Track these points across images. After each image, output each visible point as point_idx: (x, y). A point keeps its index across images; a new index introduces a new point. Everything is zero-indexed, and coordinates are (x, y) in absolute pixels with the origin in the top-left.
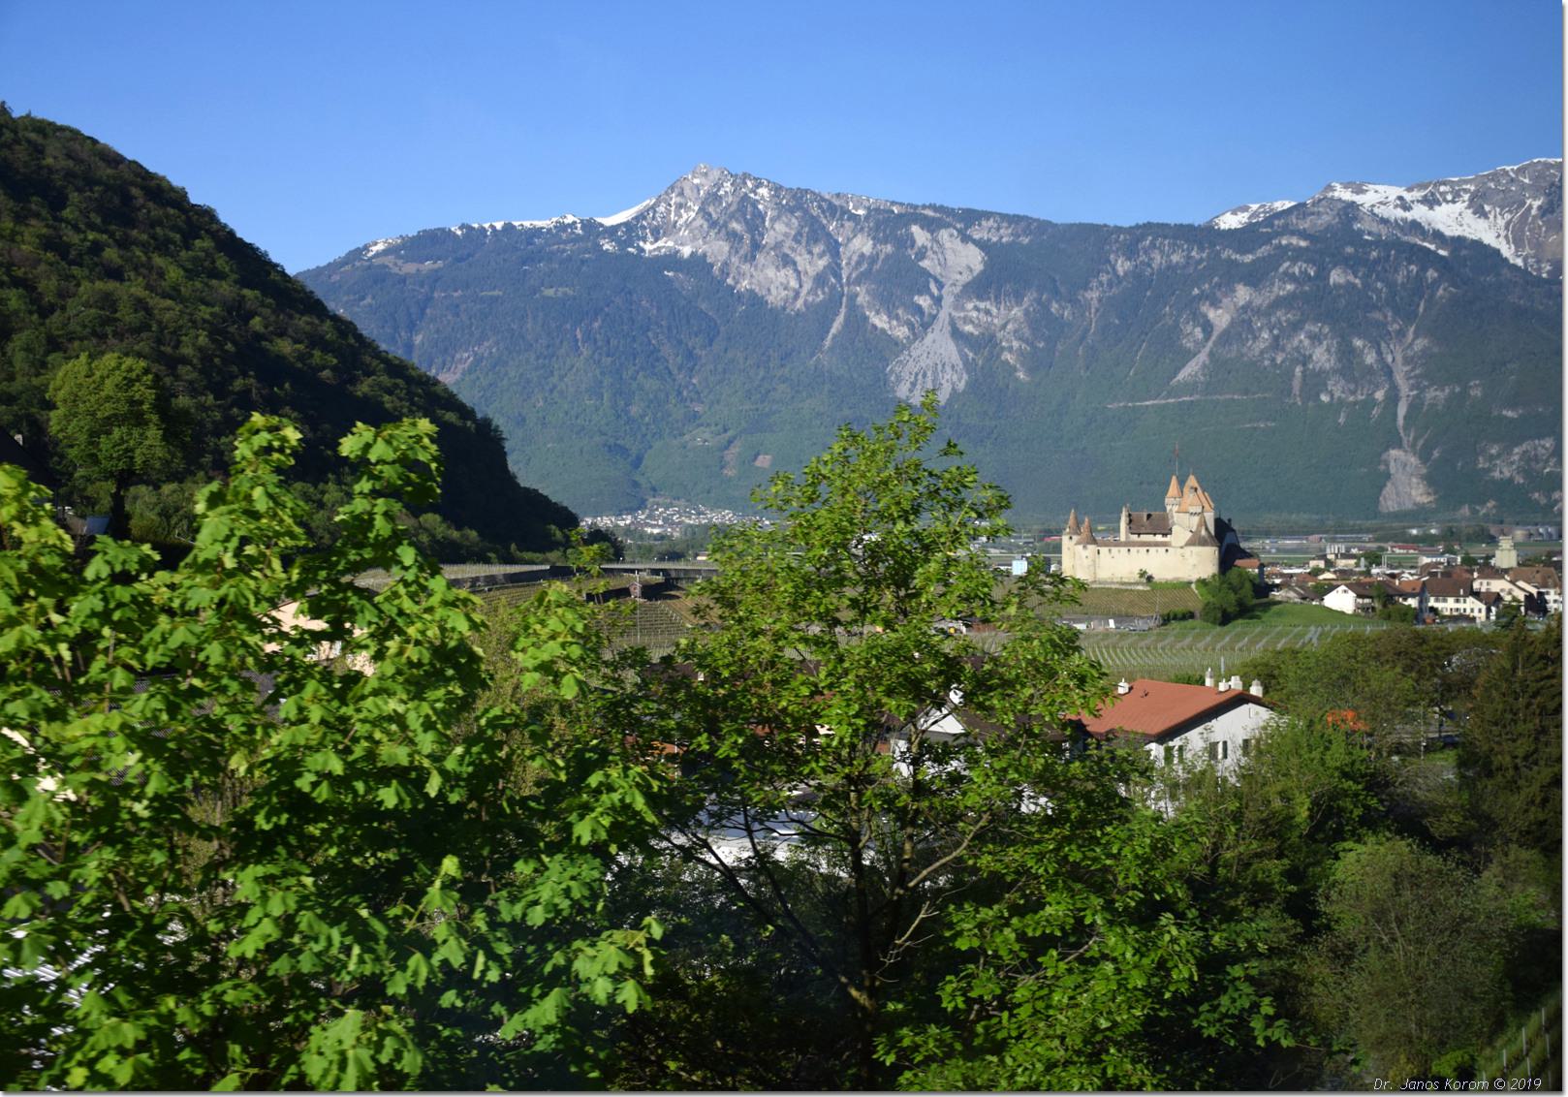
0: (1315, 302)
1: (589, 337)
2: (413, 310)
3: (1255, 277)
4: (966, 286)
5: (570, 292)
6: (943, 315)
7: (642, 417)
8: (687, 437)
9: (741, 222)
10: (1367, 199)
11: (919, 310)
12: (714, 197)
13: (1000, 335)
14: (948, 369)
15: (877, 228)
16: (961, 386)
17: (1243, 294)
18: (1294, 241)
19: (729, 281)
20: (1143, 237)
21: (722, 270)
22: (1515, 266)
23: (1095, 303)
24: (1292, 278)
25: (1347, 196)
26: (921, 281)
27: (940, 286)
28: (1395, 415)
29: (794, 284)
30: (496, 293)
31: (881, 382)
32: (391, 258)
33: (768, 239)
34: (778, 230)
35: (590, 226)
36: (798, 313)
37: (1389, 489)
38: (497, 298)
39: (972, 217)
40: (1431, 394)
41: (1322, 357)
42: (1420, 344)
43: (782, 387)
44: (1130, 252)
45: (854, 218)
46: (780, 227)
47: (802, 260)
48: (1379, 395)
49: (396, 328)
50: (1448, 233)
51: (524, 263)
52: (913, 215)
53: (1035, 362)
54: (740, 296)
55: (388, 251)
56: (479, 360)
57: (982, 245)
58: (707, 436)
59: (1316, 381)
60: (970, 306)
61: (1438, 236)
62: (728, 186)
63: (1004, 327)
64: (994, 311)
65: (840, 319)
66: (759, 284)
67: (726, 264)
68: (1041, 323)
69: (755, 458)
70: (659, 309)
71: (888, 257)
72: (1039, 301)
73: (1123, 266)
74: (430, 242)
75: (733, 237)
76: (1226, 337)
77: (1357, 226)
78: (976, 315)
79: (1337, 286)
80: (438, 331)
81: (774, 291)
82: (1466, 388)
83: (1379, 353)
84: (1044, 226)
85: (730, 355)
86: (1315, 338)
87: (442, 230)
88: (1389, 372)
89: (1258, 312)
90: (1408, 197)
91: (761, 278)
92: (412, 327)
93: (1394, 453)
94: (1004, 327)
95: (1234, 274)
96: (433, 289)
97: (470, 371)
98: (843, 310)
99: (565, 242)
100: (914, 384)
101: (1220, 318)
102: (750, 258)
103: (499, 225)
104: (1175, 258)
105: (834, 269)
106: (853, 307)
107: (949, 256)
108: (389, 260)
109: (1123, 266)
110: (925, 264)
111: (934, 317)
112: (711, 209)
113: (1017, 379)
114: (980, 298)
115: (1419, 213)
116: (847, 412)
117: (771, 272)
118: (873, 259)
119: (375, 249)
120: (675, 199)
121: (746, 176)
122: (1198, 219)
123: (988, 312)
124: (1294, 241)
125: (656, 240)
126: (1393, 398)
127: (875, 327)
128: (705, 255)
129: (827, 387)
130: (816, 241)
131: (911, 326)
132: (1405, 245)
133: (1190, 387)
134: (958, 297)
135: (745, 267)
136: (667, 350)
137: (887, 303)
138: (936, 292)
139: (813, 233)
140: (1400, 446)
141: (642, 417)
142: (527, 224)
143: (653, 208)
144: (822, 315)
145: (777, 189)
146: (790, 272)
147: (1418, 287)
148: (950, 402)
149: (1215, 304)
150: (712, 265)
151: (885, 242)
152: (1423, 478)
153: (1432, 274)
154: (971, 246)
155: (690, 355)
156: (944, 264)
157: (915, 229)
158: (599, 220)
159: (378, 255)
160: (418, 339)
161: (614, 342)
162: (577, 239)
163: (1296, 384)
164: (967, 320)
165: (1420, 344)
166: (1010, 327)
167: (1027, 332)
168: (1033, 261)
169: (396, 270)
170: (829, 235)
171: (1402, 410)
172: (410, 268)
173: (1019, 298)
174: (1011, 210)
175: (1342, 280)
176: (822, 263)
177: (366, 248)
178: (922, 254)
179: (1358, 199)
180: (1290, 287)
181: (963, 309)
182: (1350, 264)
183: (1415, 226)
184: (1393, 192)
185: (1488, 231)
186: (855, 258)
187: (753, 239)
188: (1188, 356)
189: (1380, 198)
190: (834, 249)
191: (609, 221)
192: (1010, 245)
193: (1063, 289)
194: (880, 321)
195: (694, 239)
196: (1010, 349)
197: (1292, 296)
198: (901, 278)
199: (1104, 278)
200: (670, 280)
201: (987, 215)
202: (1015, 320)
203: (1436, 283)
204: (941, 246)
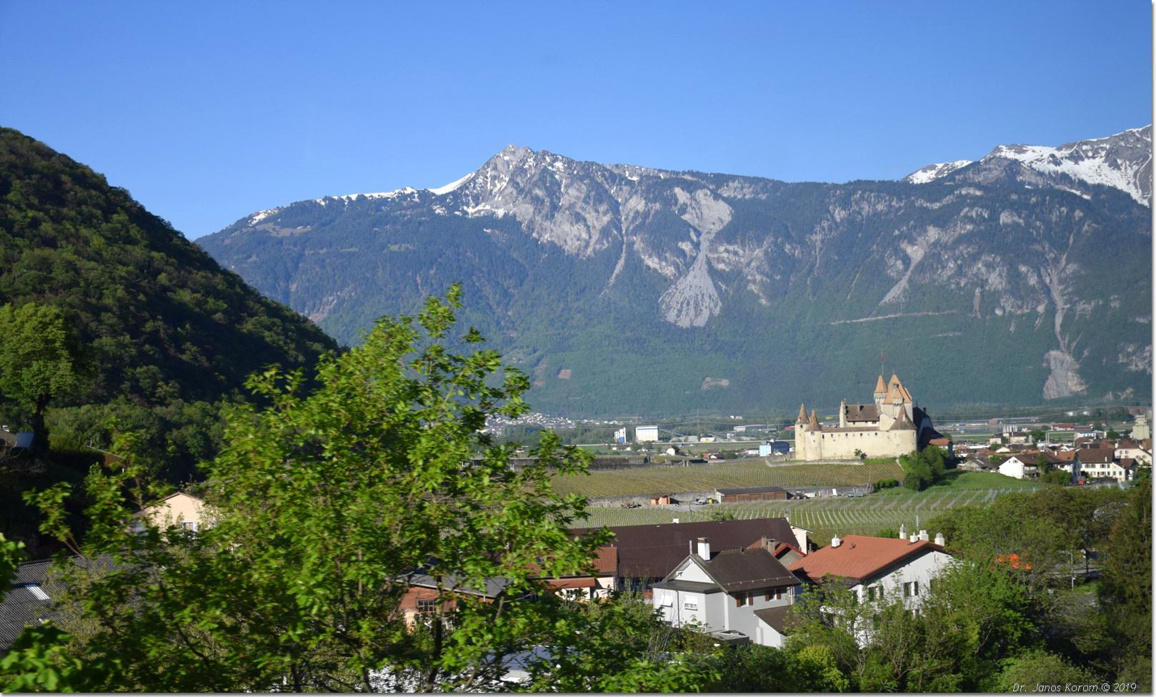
0: (989, 239)
2: (290, 265)
3: (941, 220)
4: (718, 234)
5: (411, 248)
6: (701, 256)
9: (542, 189)
10: (1026, 157)
11: (682, 253)
12: (520, 170)
13: (746, 270)
14: (707, 299)
15: (648, 191)
16: (717, 311)
17: (933, 233)
18: (971, 191)
19: (535, 235)
20: (855, 192)
21: (528, 227)
22: (1142, 206)
23: (819, 244)
24: (971, 220)
25: (1011, 155)
26: (683, 231)
27: (698, 234)
28: (1053, 324)
29: (585, 236)
30: (353, 250)
31: (654, 307)
33: (564, 202)
34: (571, 194)
35: (424, 195)
36: (589, 259)
37: (1050, 382)
38: (353, 254)
39: (720, 180)
40: (1081, 306)
41: (996, 280)
42: (1071, 268)
44: (845, 204)
45: (630, 183)
46: (572, 191)
47: (590, 217)
48: (1041, 309)
49: (276, 279)
50: (1090, 181)
52: (677, 180)
53: (775, 291)
54: (543, 245)
56: (341, 302)
57: (728, 201)
58: (521, 356)
59: (991, 299)
60: (722, 249)
61: (1082, 184)
62: (531, 161)
63: (749, 264)
64: (741, 252)
65: (621, 262)
66: (558, 237)
67: (531, 221)
68: (777, 260)
69: (559, 372)
70: (480, 258)
71: (657, 212)
72: (775, 244)
73: (839, 214)
74: (300, 212)
75: (537, 201)
76: (921, 267)
77: (1019, 178)
78: (726, 256)
79: (1006, 225)
80: (309, 280)
81: (569, 242)
82: (1107, 302)
83: (1040, 276)
84: (778, 185)
85: (536, 293)
86: (990, 267)
87: (310, 202)
88: (1048, 291)
89: (945, 247)
90: (1058, 154)
91: (559, 232)
92: (288, 278)
93: (1053, 353)
94: (749, 264)
95: (926, 219)
97: (335, 311)
99: (406, 209)
100: (680, 311)
101: (916, 252)
102: (550, 217)
103: (354, 197)
104: (880, 207)
105: (616, 223)
106: (631, 253)
107: (705, 211)
109: (839, 214)
110: (686, 217)
111: (694, 258)
112: (518, 180)
113: (760, 305)
114: (729, 243)
115: (1067, 167)
116: (628, 334)
117: (566, 227)
118: (646, 215)
119: (257, 218)
120: (490, 173)
121: (545, 153)
122: (896, 176)
123: (736, 253)
124: (971, 191)
125: (477, 205)
126: (1051, 311)
127: (648, 267)
128: (515, 216)
129: (613, 315)
130: (601, 202)
131: (677, 267)
132: (1058, 192)
133: (894, 307)
134: (712, 242)
135: (547, 224)
136: (488, 290)
137: (657, 249)
138: (695, 238)
139: (599, 195)
140: (1058, 348)
142: (376, 195)
143: (473, 180)
144: (607, 260)
145: (569, 163)
147: (1068, 225)
148: (708, 324)
149: (912, 242)
150: (521, 223)
151: (655, 201)
152: (1077, 372)
153: (1078, 214)
154: (721, 203)
155: (506, 293)
156: (700, 217)
157: (677, 190)
158: (432, 190)
159: (260, 222)
160: (293, 287)
162: (416, 205)
163: (977, 302)
164: (720, 260)
165: (1071, 268)
166: (753, 264)
167: (767, 268)
168: (773, 212)
169: (274, 234)
170: (611, 197)
171: (1059, 320)
172: (286, 232)
173: (760, 243)
174: (751, 175)
175: (1009, 221)
176: (606, 219)
177: (251, 217)
178: (683, 210)
179: (1020, 157)
180: (969, 227)
181: (716, 251)
182: (1015, 207)
183: (1064, 177)
184: (1047, 151)
185: (1121, 180)
186: (632, 214)
187: (552, 202)
188: (892, 282)
189: (1036, 156)
190: (615, 207)
191: (439, 191)
192: (751, 200)
193: (793, 234)
194: (652, 262)
195: (506, 203)
196: (754, 282)
197: (971, 234)
198: (667, 229)
199: (825, 224)
200: (489, 236)
201: (733, 178)
202: (757, 258)
203: (1082, 220)
204: (698, 203)
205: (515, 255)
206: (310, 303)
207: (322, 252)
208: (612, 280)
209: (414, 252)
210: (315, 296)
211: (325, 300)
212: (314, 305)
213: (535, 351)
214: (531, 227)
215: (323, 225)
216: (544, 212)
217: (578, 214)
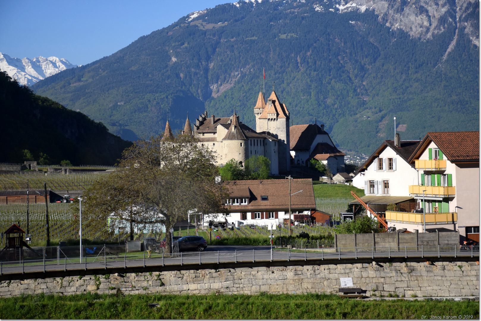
1: (304, 60)
2: (210, 49)
5: (295, 36)
7: (333, 105)
8: (358, 116)
19: (388, 24)
21: (383, 19)
29: (426, 23)
30: (253, 38)
32: (200, 21)
36: (428, 41)
38: (254, 41)
43: (416, 84)
49: (200, 60)
51: (271, 21)
54: (393, 33)
55: (201, 17)
56: (243, 76)
58: (369, 114)
65: (454, 43)
66: (406, 25)
67: (386, 15)
70: (345, 43)
80: (222, 61)
81: (414, 29)
85: (385, 67)
87: (229, 4)
91: (407, 21)
92: (208, 59)
96: (220, 38)
97: (239, 82)
98: (456, 37)
99: (295, 8)
102: (400, 10)
105: (452, 13)
106: (462, 34)
108: (197, 23)
116: (454, 97)
117: (412, 18)
119: (192, 17)
125: (346, 4)
135: (397, 16)
136: (349, 66)
141: (333, 105)
144: (442, 41)
146: (424, 17)
155: (362, 68)
159: (194, 20)
160: (211, 65)
161: (318, 63)
169: (202, 28)
172: (210, 26)
176: (444, 10)
177: (188, 17)
186: (465, 5)
200: (353, 26)
205: (371, 40)
206: (222, 77)
207: (232, 40)
208: (445, 57)
209: (297, 39)
210: (226, 71)
211: (232, 74)
212: (225, 78)
213: (380, 111)
214: (385, 20)
215: (236, 21)
216: (396, 7)
217: (422, 7)
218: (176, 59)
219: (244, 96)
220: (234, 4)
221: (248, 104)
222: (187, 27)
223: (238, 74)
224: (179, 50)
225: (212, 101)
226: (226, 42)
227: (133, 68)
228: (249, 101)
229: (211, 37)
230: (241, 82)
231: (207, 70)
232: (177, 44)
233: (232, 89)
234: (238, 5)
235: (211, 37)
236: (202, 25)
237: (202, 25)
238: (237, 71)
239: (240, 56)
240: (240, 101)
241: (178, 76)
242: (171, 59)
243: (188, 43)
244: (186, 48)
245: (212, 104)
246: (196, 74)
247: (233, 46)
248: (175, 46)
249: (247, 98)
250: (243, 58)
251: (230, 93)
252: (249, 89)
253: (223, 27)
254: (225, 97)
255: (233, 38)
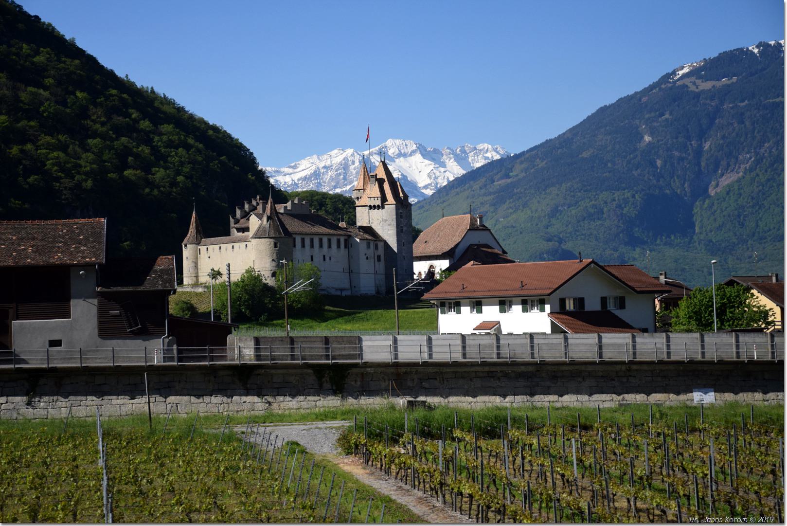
32: (693, 79)
55: (695, 73)
56: (758, 162)
80: (723, 137)
87: (740, 50)
92: (702, 135)
97: (751, 170)
108: (687, 81)
119: (681, 73)
159: (685, 76)
160: (707, 146)
169: (693, 88)
172: (707, 85)
177: (674, 73)
206: (724, 163)
211: (741, 157)
212: (728, 165)
218: (650, 138)
219: (760, 191)
220: (750, 48)
221: (765, 203)
222: (671, 88)
223: (751, 158)
224: (655, 124)
225: (707, 201)
226: (732, 108)
227: (585, 155)
228: (769, 199)
229: (708, 102)
230: (755, 169)
231: (699, 152)
232: (653, 114)
233: (739, 180)
234: (756, 51)
235: (708, 102)
236: (694, 83)
237: (694, 83)
238: (747, 153)
239: (754, 129)
240: (753, 198)
241: (653, 164)
242: (642, 137)
243: (671, 114)
244: (667, 120)
245: (706, 206)
246: (681, 159)
247: (742, 114)
248: (649, 118)
249: (764, 194)
250: (759, 132)
251: (736, 187)
252: (768, 180)
253: (728, 86)
254: (728, 193)
255: (743, 101)
